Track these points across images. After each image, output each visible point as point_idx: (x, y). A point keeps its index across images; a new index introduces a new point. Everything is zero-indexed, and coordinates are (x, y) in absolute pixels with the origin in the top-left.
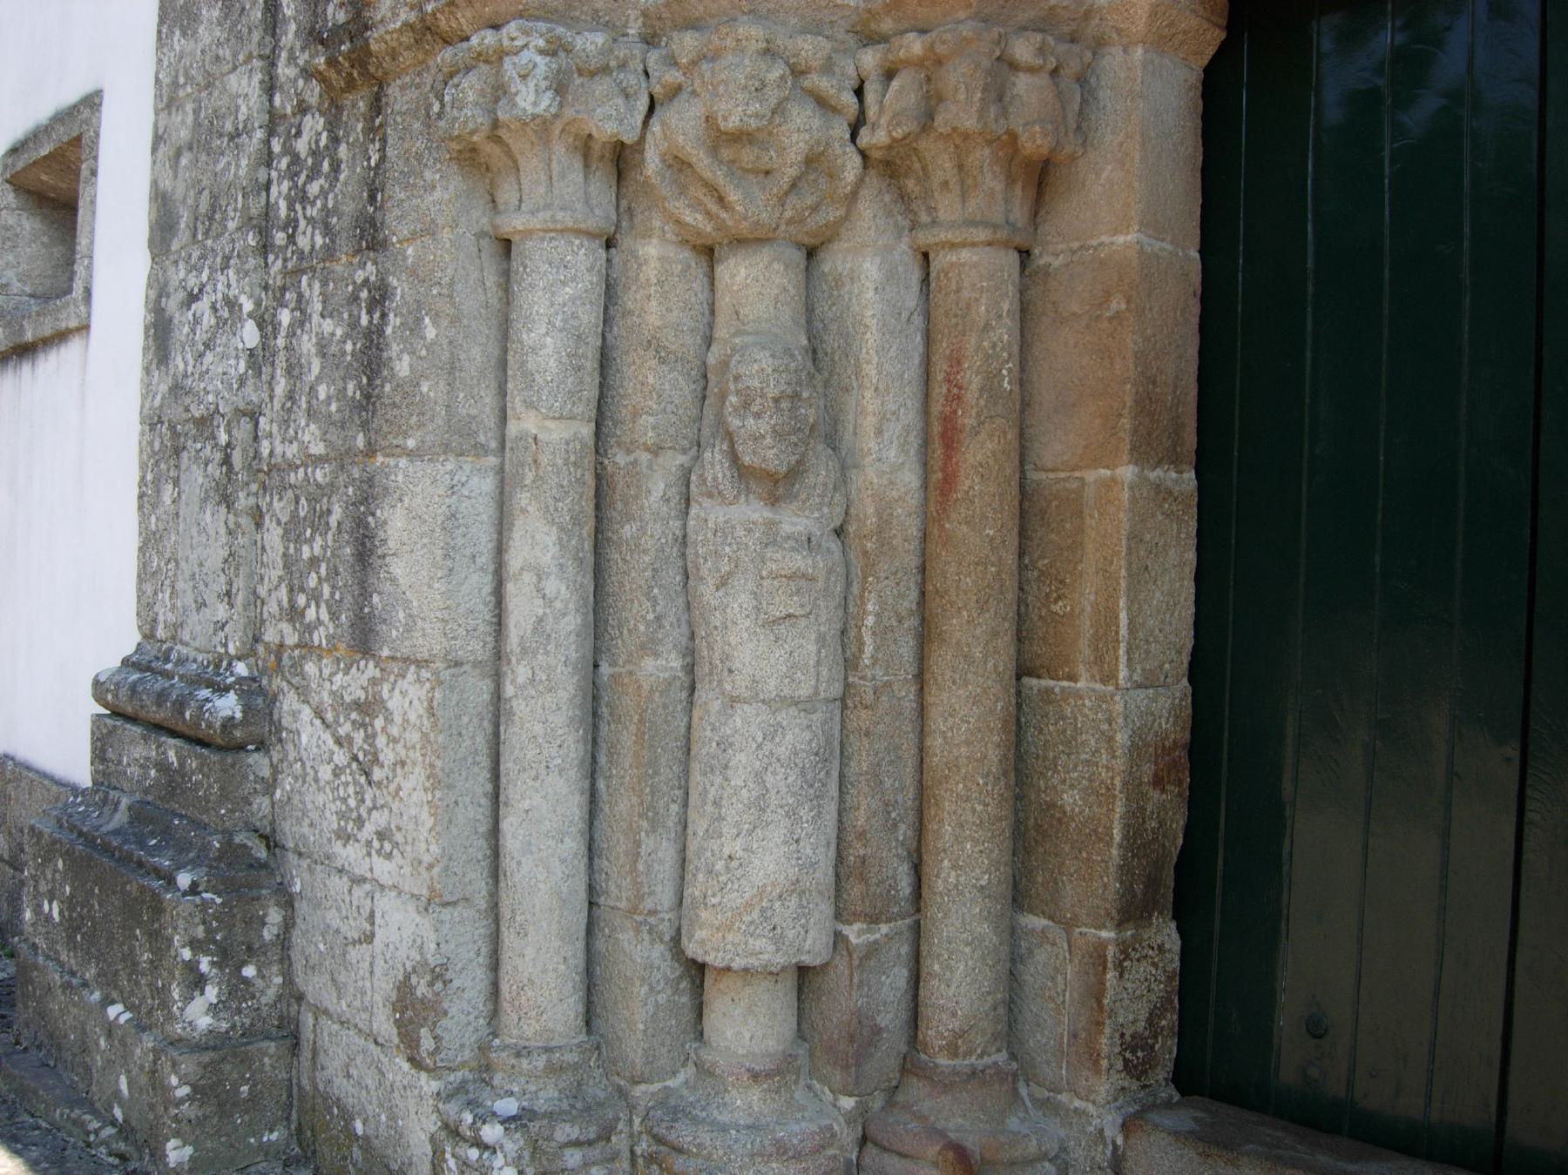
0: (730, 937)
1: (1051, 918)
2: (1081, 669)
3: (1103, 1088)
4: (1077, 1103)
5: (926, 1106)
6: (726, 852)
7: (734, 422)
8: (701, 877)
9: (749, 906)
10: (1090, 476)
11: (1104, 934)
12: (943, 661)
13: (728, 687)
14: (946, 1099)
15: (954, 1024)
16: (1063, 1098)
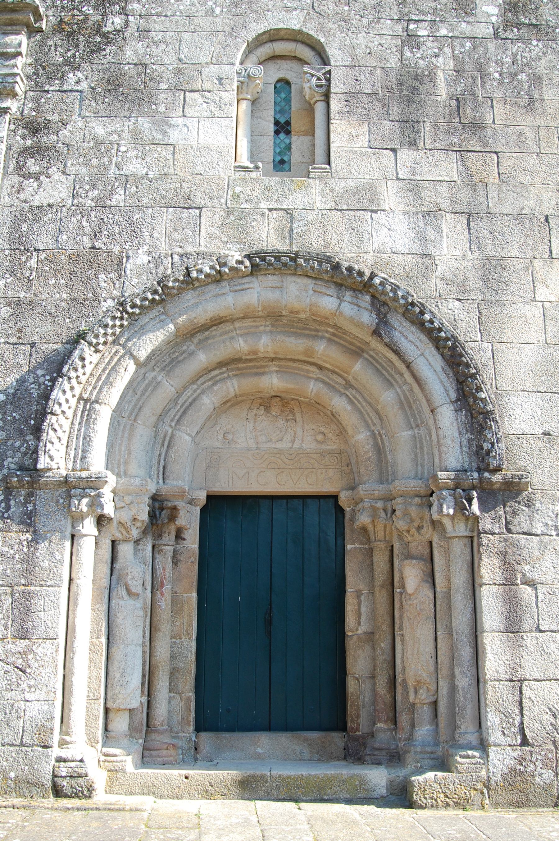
0: (127, 700)
1: (176, 693)
2: (183, 637)
3: (192, 728)
4: (184, 734)
5: (158, 739)
6: (126, 680)
7: (130, 582)
8: (118, 687)
9: (132, 692)
10: (185, 595)
11: (190, 694)
12: (159, 636)
13: (126, 642)
14: (162, 736)
15: (162, 718)
16: (180, 734)
